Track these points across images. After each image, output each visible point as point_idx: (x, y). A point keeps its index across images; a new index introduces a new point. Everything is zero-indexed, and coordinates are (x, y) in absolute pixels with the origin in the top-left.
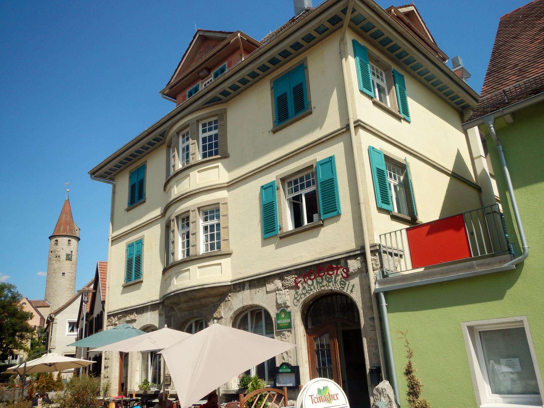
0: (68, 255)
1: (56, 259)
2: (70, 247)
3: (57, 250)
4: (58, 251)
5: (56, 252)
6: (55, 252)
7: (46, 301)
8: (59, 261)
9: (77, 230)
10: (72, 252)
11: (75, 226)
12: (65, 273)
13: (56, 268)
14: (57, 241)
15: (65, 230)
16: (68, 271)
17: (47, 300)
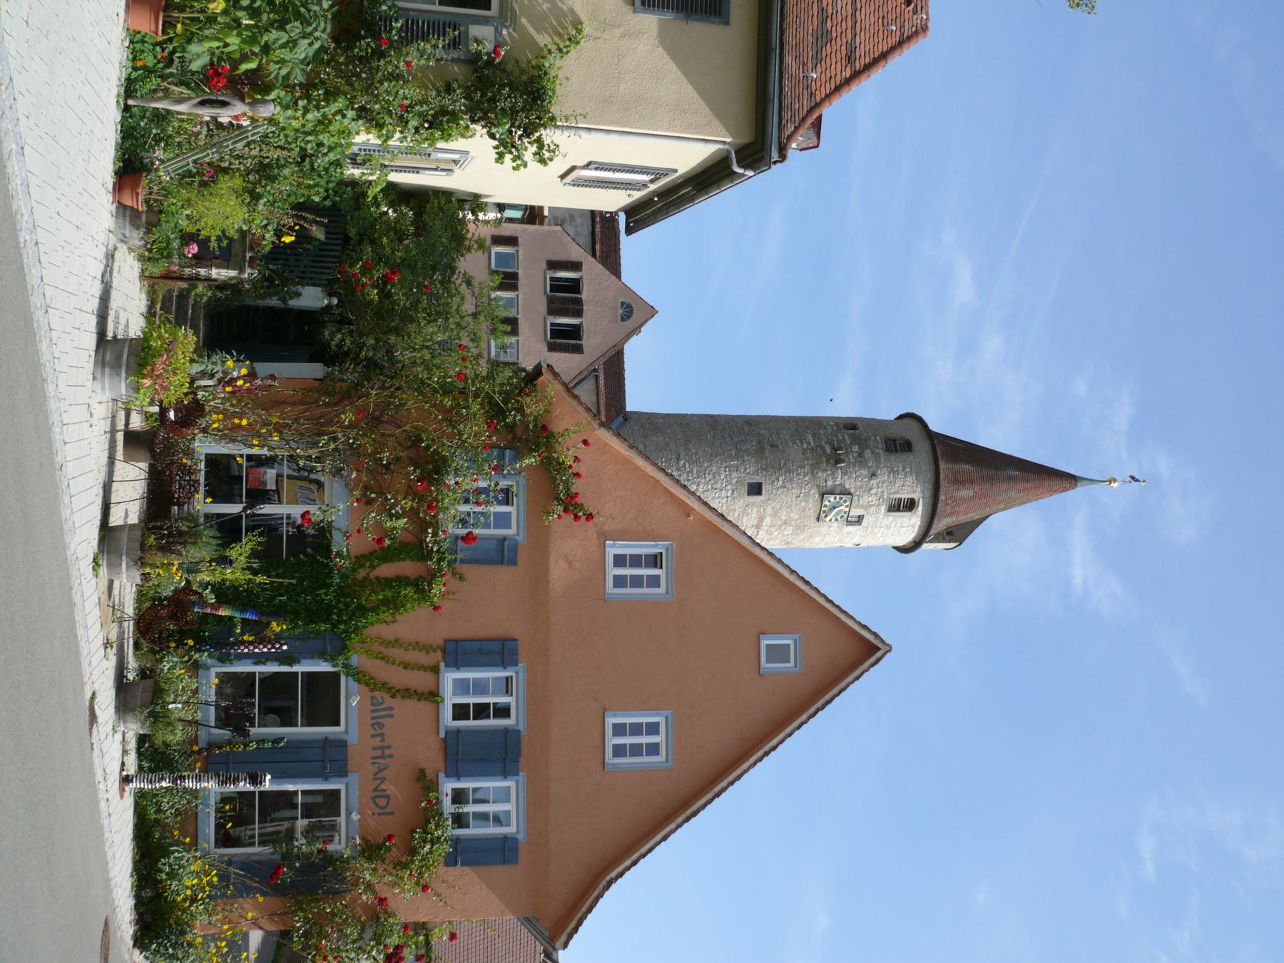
1: (823, 449)
3: (868, 453)
4: (861, 455)
6: (855, 440)
7: (621, 419)
13: (784, 452)
14: (907, 447)
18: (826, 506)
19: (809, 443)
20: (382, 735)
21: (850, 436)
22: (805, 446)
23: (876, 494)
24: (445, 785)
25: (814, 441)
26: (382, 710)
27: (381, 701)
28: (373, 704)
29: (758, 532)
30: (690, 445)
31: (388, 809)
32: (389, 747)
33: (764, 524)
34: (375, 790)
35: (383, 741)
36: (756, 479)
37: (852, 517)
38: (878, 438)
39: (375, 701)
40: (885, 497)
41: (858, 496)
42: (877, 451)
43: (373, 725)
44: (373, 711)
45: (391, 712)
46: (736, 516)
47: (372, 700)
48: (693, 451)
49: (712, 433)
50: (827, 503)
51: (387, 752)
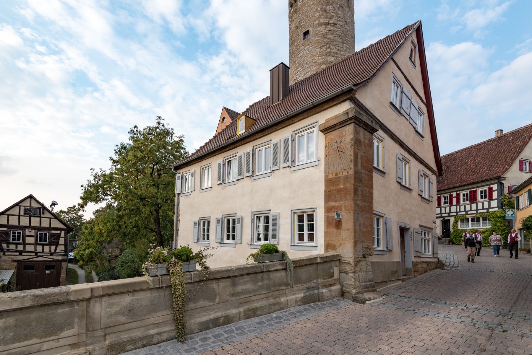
16: (317, 22)
46: (320, 38)
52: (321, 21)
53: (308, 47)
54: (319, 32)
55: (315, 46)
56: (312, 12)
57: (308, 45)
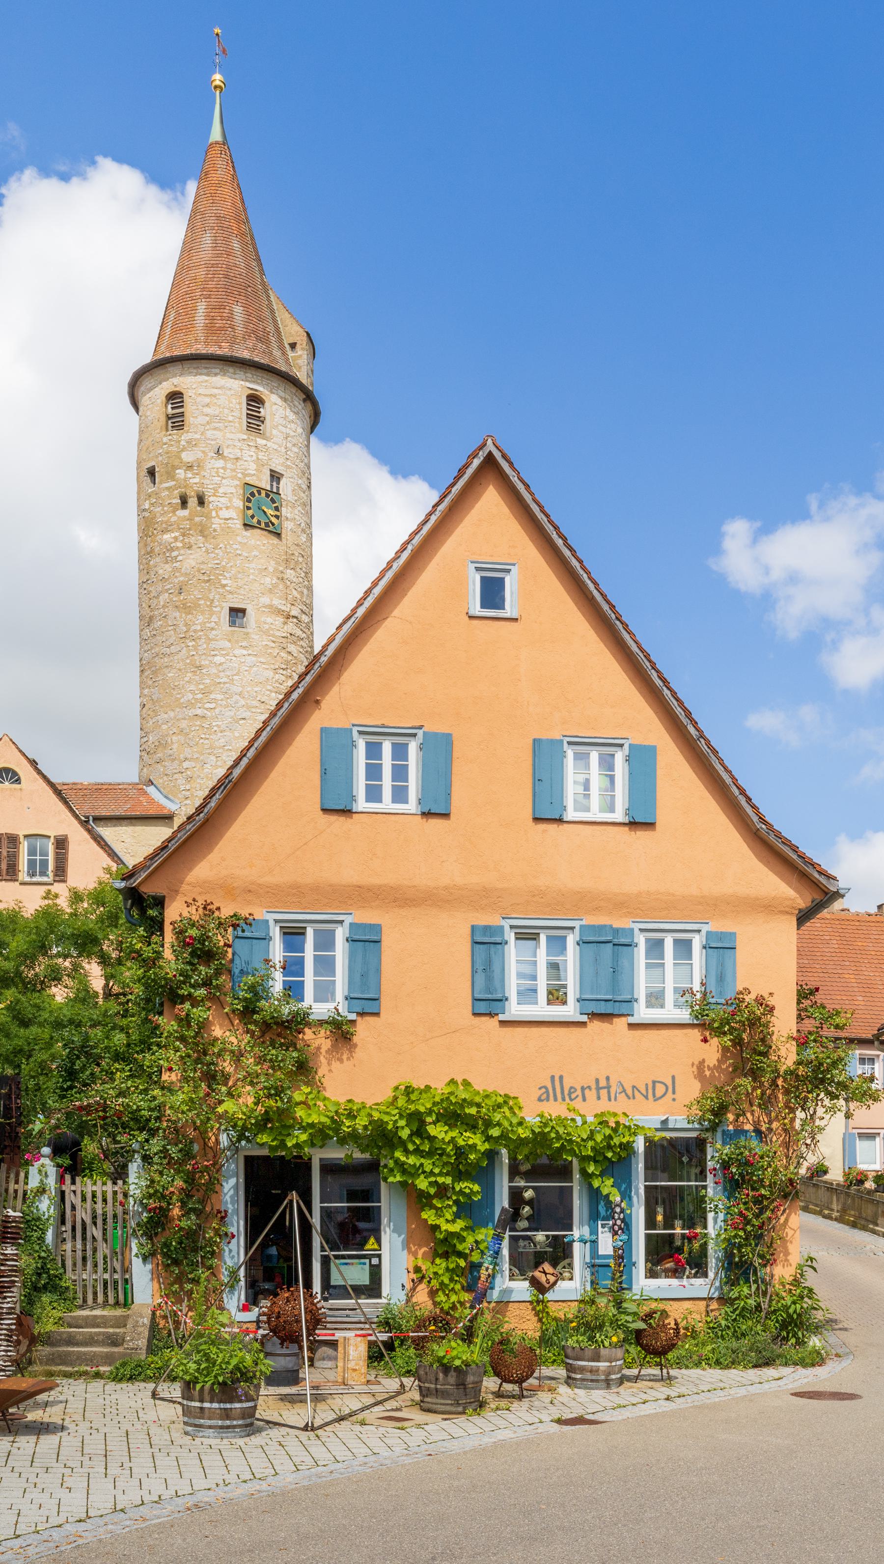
0: (251, 493)
2: (261, 441)
3: (187, 457)
4: (190, 467)
5: (180, 473)
6: (171, 475)
8: (203, 531)
9: (293, 346)
10: (275, 477)
11: (282, 316)
12: (243, 611)
14: (175, 397)
15: (221, 329)
16: (265, 600)
17: (152, 783)
18: (259, 522)
19: (176, 539)
20: (583, 1089)
21: (161, 483)
22: (179, 544)
23: (241, 450)
24: (642, 1016)
25: (172, 531)
26: (554, 1089)
27: (543, 1090)
28: (548, 1099)
29: (294, 617)
30: (182, 700)
31: (670, 1084)
32: (597, 1081)
33: (283, 608)
34: (646, 1097)
35: (589, 1087)
36: (225, 614)
37: (272, 486)
38: (165, 440)
39: (545, 1095)
40: (245, 437)
41: (245, 475)
42: (183, 443)
43: (571, 1100)
44: (556, 1099)
45: (557, 1079)
46: (273, 645)
47: (542, 1101)
48: (190, 696)
49: (166, 671)
50: (255, 520)
51: (603, 1083)
52: (277, 602)
53: (245, 652)
54: (272, 629)
55: (262, 660)
56: (253, 565)
57: (245, 648)
